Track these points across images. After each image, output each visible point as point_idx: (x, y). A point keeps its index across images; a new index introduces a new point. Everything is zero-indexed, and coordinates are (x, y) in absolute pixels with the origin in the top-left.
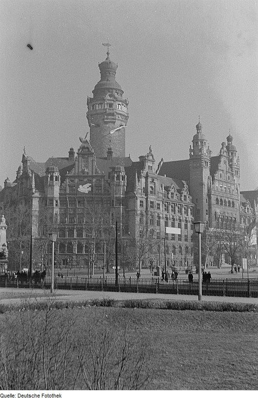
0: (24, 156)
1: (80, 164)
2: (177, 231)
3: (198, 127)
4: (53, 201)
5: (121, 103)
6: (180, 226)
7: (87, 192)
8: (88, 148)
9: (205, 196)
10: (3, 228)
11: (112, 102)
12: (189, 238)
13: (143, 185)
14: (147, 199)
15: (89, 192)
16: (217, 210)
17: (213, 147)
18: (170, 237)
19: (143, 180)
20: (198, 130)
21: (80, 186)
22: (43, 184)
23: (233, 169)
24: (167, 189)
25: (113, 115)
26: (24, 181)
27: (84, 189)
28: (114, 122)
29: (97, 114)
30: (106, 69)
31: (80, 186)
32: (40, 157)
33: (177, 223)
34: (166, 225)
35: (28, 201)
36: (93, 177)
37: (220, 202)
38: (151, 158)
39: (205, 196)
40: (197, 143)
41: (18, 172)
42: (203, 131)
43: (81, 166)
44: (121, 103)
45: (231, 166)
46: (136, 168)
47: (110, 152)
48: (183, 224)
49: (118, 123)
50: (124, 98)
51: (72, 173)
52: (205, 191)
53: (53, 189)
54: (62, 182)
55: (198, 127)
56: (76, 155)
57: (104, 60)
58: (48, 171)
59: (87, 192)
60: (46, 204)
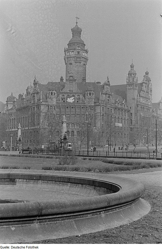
0: (35, 81)
2: (120, 125)
3: (132, 66)
5: (84, 51)
7: (72, 102)
8: (73, 77)
10: (65, 122)
11: (80, 50)
15: (73, 102)
17: (140, 79)
21: (68, 99)
23: (149, 91)
25: (80, 58)
27: (71, 100)
28: (80, 63)
29: (71, 57)
30: (77, 32)
31: (68, 99)
32: (44, 82)
38: (108, 83)
40: (131, 75)
44: (84, 51)
47: (84, 79)
48: (123, 121)
50: (86, 49)
51: (64, 91)
55: (132, 66)
56: (64, 81)
57: (73, 26)
59: (72, 102)
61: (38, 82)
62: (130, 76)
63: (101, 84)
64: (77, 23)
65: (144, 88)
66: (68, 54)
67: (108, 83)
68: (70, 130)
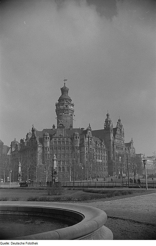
1: (59, 132)
2: (101, 161)
3: (107, 115)
4: (47, 148)
5: (71, 105)
6: (102, 159)
8: (62, 125)
9: (112, 145)
12: (106, 164)
13: (87, 141)
14: (89, 147)
16: (117, 151)
18: (98, 163)
19: (87, 138)
20: (107, 116)
22: (42, 141)
24: (96, 143)
25: (68, 110)
26: (33, 139)
28: (68, 114)
29: (61, 110)
30: (64, 90)
32: (39, 128)
33: (100, 157)
34: (96, 157)
35: (36, 148)
36: (65, 137)
37: (117, 148)
38: (90, 129)
39: (112, 145)
41: (27, 136)
42: (110, 117)
43: (59, 132)
44: (71, 105)
45: (121, 132)
46: (84, 132)
47: (71, 126)
48: (103, 158)
49: (70, 114)
50: (72, 103)
51: (55, 135)
52: (112, 143)
53: (46, 143)
54: (51, 140)
56: (56, 128)
58: (44, 135)
60: (44, 150)
61: (35, 130)
62: (106, 123)
63: (85, 130)
64: (65, 84)
65: (118, 132)
66: (58, 107)
67: (90, 129)
68: (61, 167)
